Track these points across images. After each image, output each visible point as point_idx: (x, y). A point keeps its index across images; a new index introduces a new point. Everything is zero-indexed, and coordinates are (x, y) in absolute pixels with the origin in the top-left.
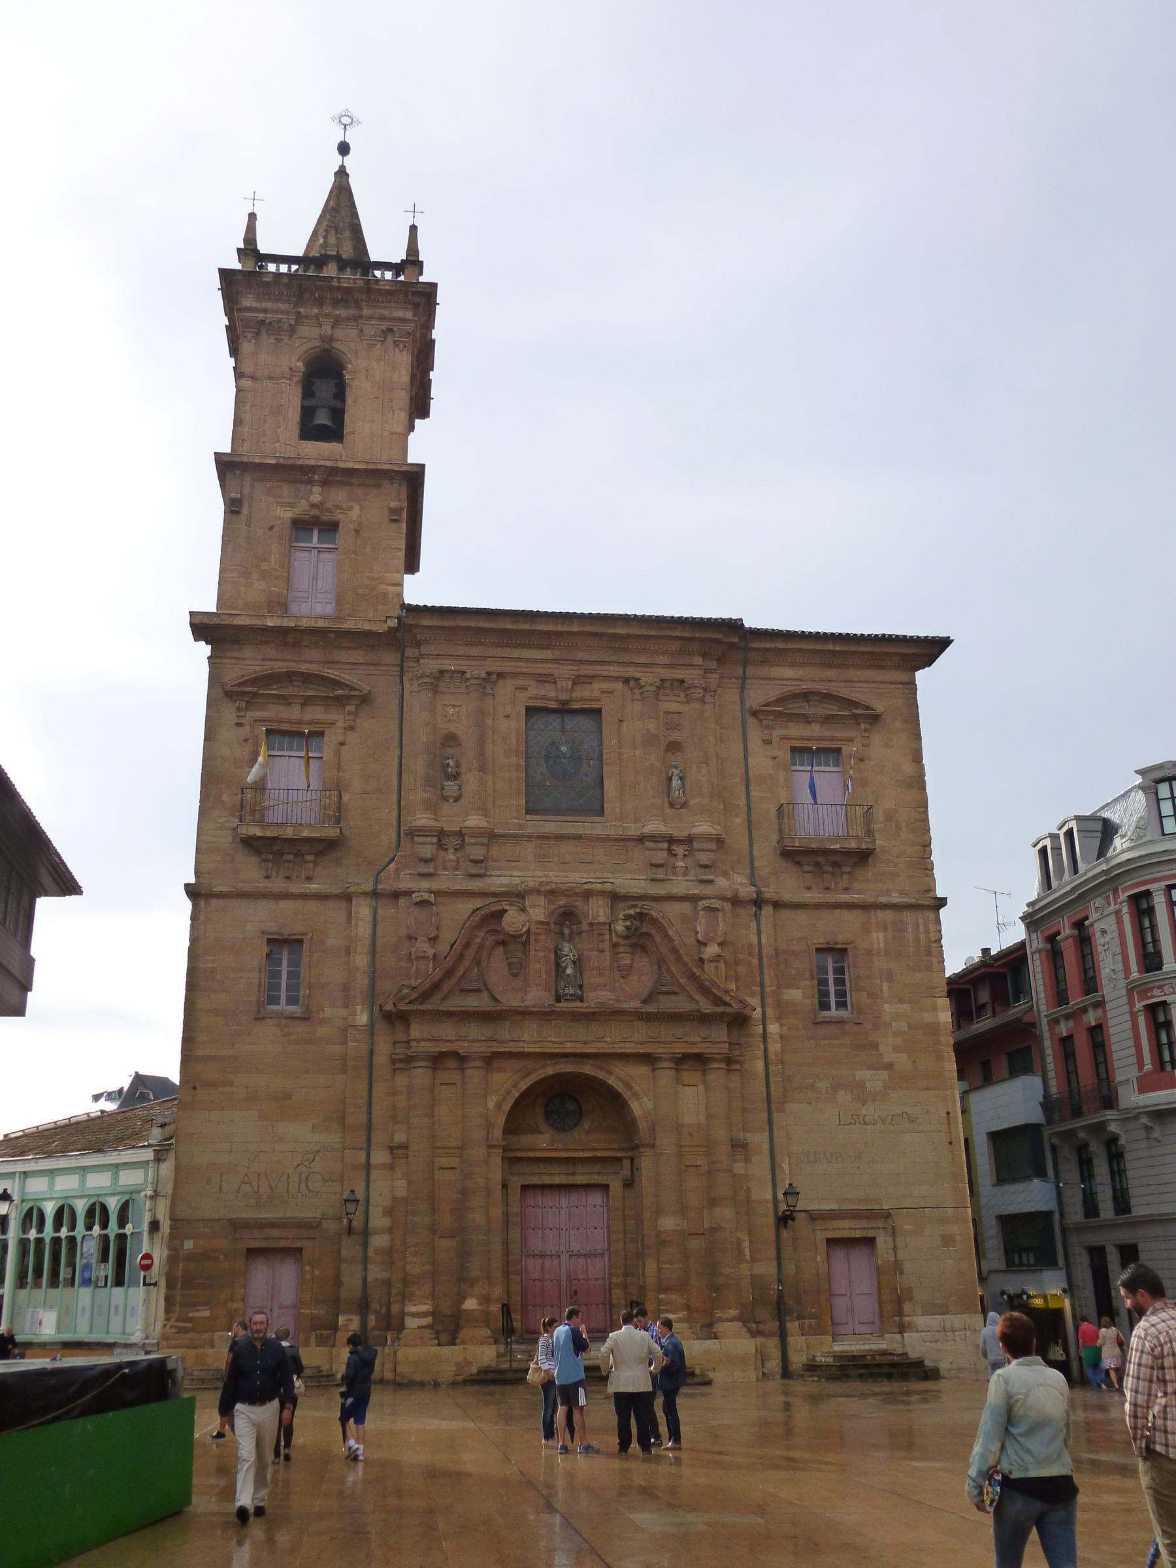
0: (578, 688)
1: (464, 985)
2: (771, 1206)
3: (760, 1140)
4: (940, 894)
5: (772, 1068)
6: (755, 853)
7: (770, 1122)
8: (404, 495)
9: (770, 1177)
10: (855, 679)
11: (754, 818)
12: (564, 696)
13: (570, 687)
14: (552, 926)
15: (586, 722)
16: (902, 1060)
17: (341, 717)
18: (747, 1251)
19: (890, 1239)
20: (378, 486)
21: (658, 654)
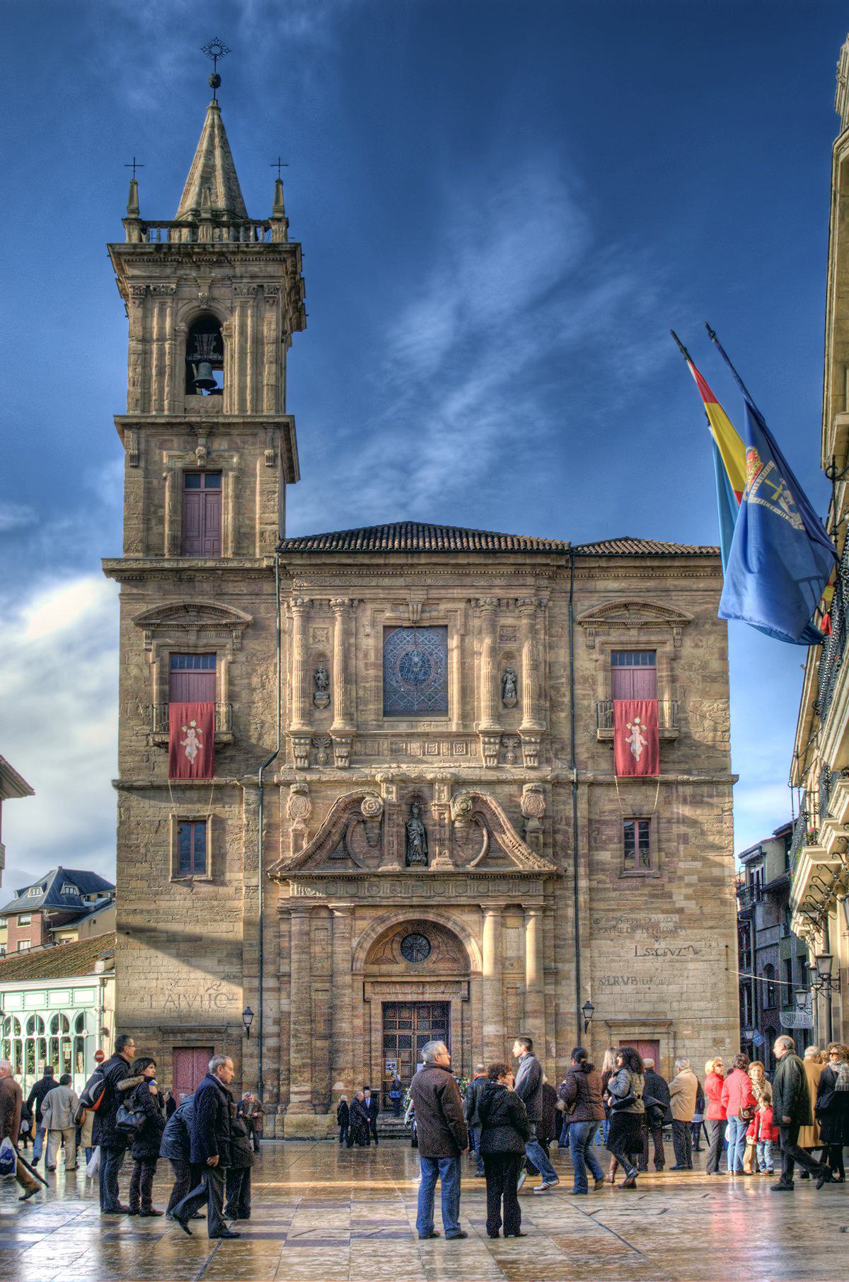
0: (427, 608)
1: (334, 855)
2: (575, 1017)
3: (570, 968)
4: (734, 772)
5: (581, 915)
6: (578, 742)
7: (578, 955)
8: (279, 443)
9: (574, 996)
10: (672, 588)
11: (578, 711)
12: (416, 617)
13: (419, 609)
14: (404, 807)
15: (433, 636)
16: (691, 906)
17: (230, 640)
18: (554, 1050)
19: (672, 1041)
20: (255, 435)
21: (495, 577)
